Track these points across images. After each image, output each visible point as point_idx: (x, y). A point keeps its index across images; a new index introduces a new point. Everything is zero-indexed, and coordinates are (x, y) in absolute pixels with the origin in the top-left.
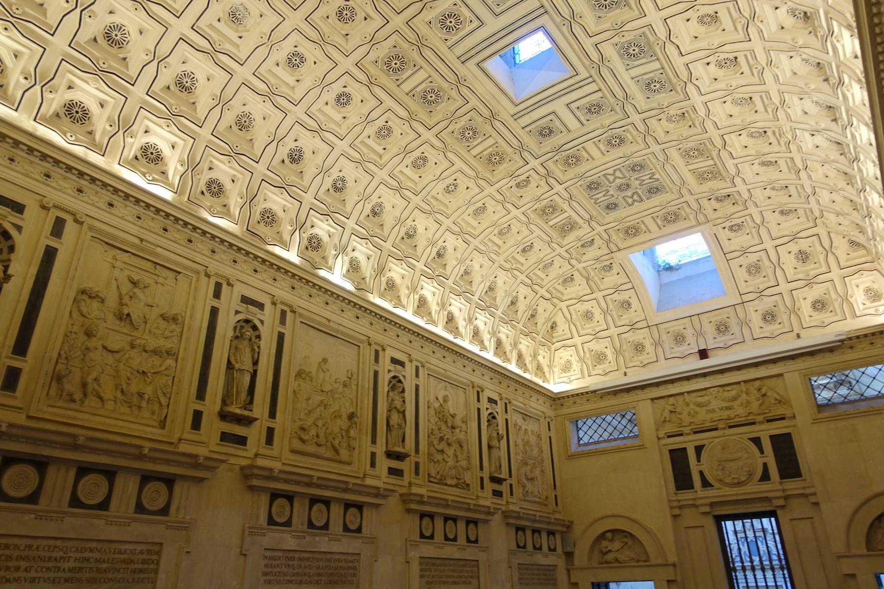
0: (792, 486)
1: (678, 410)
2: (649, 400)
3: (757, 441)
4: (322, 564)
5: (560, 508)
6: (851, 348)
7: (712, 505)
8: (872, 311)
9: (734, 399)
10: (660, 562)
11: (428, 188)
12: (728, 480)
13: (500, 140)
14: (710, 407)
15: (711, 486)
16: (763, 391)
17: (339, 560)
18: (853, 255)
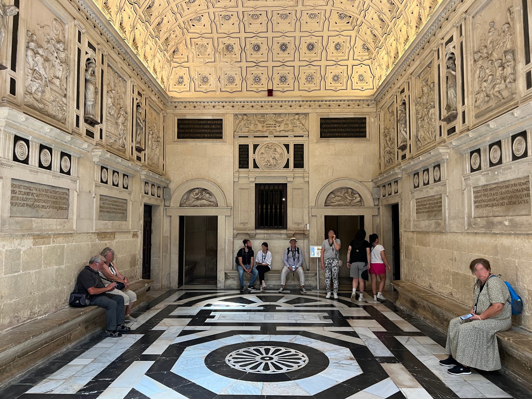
4: (503, 190)
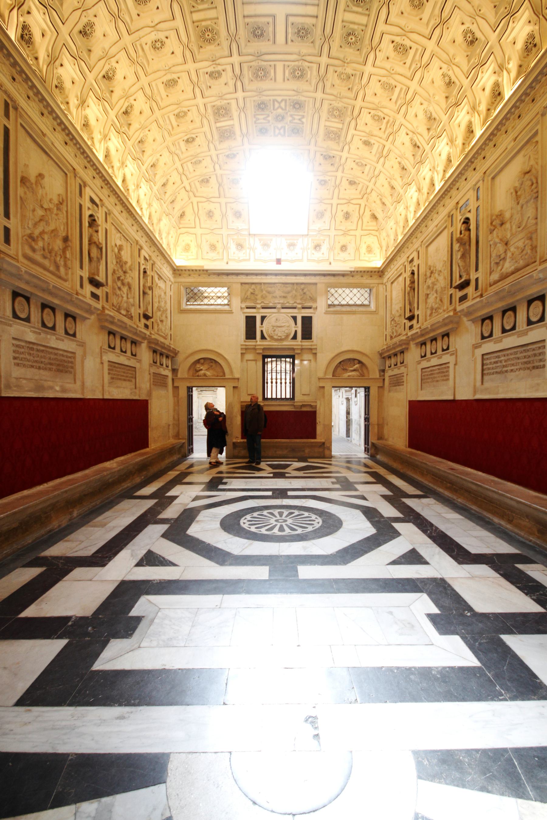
0: (306, 343)
1: (256, 293)
2: (240, 285)
3: (295, 318)
4: (52, 356)
5: (172, 342)
6: (353, 276)
7: (264, 349)
8: (367, 259)
9: (289, 292)
10: (231, 377)
11: (141, 33)
12: (276, 337)
13: (222, 18)
14: (274, 295)
15: (266, 339)
16: (305, 291)
17: (63, 355)
18: (370, 224)
